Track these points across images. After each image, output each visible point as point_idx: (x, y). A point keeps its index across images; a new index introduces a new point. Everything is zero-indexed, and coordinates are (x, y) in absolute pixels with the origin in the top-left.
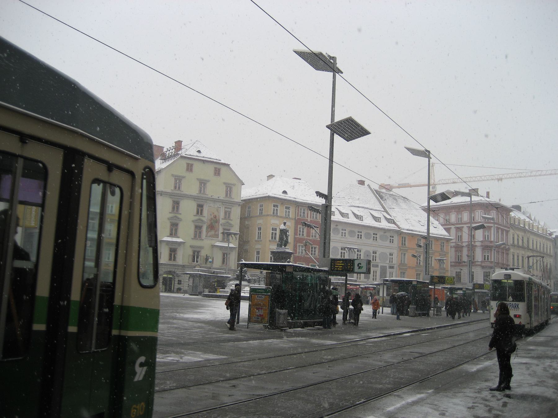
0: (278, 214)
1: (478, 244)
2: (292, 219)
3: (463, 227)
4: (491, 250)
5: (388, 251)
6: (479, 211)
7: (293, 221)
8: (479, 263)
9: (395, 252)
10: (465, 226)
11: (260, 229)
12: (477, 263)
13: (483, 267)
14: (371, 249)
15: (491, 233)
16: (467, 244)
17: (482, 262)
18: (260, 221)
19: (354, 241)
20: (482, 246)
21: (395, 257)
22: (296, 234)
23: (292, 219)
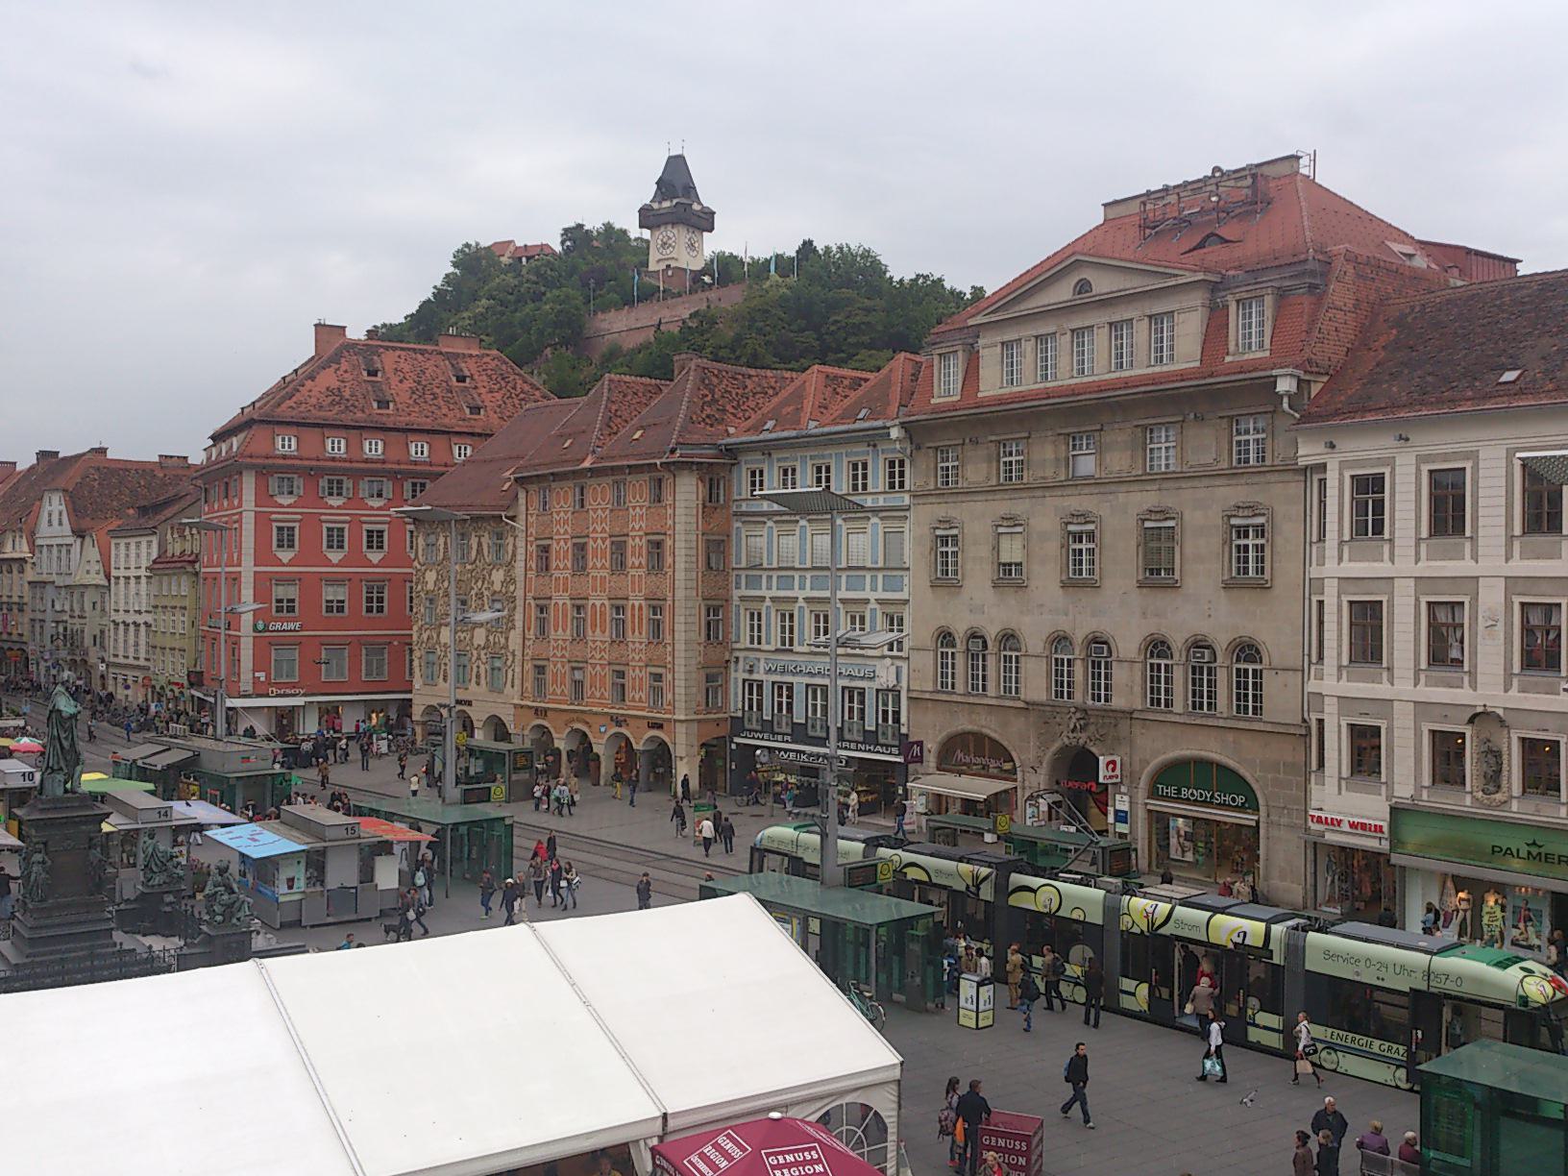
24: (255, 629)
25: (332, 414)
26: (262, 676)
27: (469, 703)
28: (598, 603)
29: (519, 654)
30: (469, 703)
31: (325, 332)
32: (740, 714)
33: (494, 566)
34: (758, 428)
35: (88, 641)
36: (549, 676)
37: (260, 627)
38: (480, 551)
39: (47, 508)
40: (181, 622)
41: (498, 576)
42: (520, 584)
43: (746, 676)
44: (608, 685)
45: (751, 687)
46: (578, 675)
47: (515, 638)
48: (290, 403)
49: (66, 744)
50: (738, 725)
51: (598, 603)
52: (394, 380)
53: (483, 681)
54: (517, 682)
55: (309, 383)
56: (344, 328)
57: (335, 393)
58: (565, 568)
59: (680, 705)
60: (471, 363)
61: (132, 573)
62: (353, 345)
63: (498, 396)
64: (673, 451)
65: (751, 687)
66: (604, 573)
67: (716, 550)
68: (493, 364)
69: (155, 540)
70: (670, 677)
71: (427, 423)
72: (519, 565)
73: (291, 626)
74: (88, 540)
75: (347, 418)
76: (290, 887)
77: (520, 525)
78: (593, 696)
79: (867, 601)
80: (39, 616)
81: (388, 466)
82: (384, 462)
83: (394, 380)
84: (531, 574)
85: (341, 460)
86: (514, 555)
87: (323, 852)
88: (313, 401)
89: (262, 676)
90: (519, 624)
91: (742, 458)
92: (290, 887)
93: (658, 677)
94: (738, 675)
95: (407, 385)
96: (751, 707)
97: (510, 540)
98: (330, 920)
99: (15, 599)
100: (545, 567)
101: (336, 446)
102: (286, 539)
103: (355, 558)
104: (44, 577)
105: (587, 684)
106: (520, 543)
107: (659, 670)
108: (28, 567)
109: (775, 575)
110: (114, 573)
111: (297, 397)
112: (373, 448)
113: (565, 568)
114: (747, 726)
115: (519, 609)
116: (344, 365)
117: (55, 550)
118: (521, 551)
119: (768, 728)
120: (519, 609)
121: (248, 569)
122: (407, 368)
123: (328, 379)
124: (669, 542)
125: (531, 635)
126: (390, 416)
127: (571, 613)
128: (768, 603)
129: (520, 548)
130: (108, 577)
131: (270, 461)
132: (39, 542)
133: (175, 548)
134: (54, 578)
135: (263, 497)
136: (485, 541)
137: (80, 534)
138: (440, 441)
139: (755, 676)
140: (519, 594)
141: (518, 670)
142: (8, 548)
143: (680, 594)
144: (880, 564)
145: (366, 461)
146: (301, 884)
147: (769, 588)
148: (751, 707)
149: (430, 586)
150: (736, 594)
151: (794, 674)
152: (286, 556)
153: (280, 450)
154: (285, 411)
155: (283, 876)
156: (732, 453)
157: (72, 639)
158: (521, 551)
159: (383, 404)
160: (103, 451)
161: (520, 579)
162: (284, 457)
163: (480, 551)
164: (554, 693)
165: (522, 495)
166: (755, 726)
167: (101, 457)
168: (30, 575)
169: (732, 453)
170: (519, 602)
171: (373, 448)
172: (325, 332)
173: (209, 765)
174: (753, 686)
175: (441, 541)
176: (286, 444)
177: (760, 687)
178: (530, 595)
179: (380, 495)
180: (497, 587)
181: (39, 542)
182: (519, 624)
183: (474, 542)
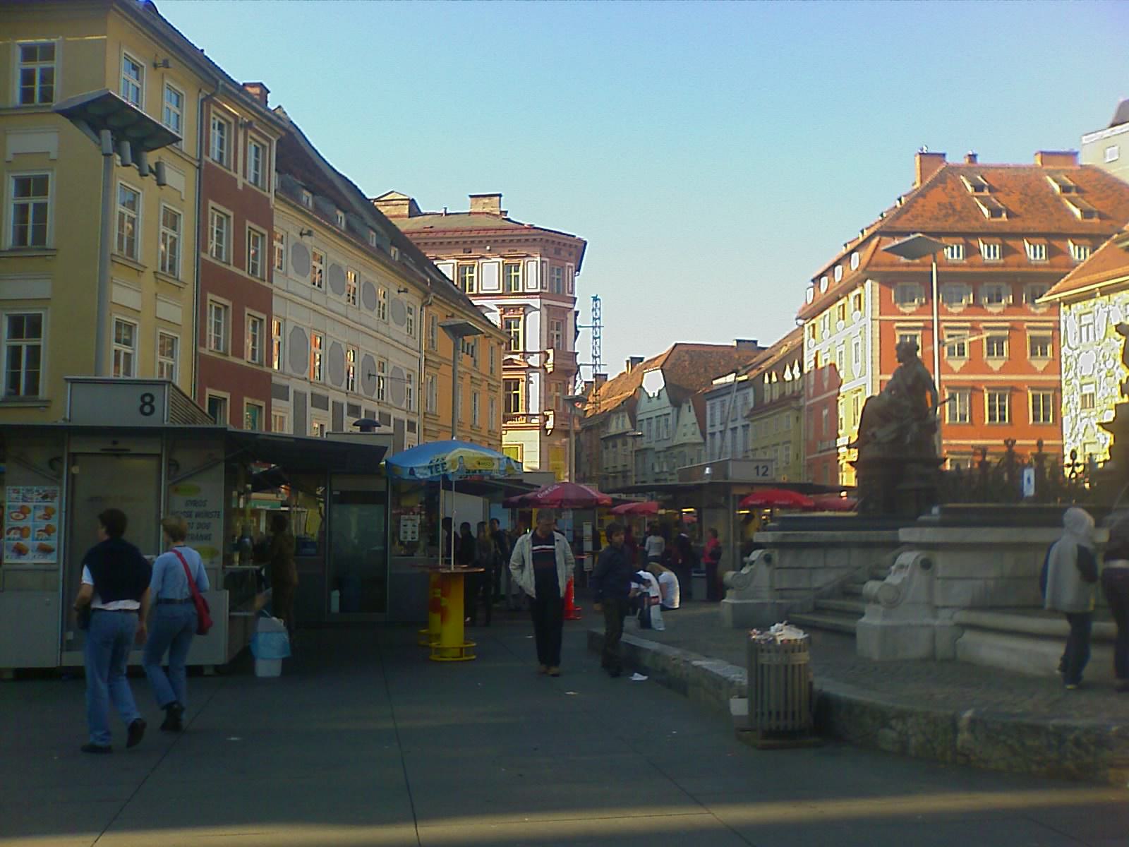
25: (948, 225)
48: (904, 217)
55: (921, 200)
56: (944, 155)
62: (955, 170)
74: (685, 407)
75: (962, 227)
81: (1009, 269)
82: (1003, 266)
99: (620, 468)
110: (709, 430)
117: (654, 420)
130: (703, 434)
132: (639, 418)
134: (653, 445)
181: (639, 418)
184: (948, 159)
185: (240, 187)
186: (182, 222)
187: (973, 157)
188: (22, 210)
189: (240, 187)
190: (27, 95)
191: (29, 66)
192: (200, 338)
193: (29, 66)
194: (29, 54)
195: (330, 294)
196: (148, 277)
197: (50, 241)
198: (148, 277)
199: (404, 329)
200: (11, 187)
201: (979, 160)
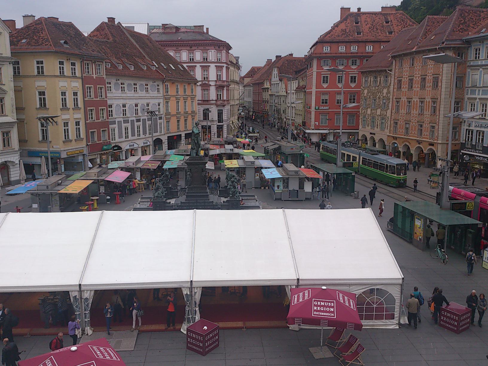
0: (65, 74)
1: (212, 83)
2: (79, 78)
3: (196, 66)
4: (223, 90)
5: (156, 101)
6: (213, 51)
7: (80, 80)
8: (214, 102)
9: (161, 101)
10: (198, 65)
11: (42, 93)
12: (212, 102)
13: (217, 106)
14: (145, 102)
15: (222, 72)
16: (200, 83)
17: (216, 100)
18: (41, 83)
19: (132, 95)
20: (215, 85)
21: (161, 105)
22: (84, 96)
23: (79, 78)
24: (315, 109)
25: (341, 39)
26: (317, 123)
27: (374, 134)
28: (415, 100)
29: (390, 118)
30: (374, 134)
31: (344, 10)
32: (464, 142)
33: (384, 87)
34: (479, 32)
35: (282, 112)
36: (398, 126)
37: (317, 108)
38: (380, 83)
39: (274, 73)
40: (300, 107)
41: (385, 91)
42: (392, 94)
43: (468, 128)
44: (404, 128)
45: (469, 132)
46: (407, 126)
47: (389, 112)
48: (329, 35)
49: (196, 142)
50: (463, 146)
51: (415, 100)
52: (364, 25)
53: (379, 127)
54: (389, 128)
57: (344, 31)
58: (418, 87)
59: (440, 138)
60: (392, 16)
61: (293, 91)
62: (353, 14)
63: (400, 27)
64: (443, 43)
65: (469, 132)
66: (418, 89)
67: (460, 81)
68: (400, 16)
69: (297, 81)
70: (437, 127)
71: (373, 39)
72: (392, 87)
73: (326, 108)
75: (347, 39)
76: (278, 188)
77: (393, 73)
78: (412, 133)
79: (476, 99)
80: (271, 104)
82: (357, 53)
83: (364, 25)
84: (395, 90)
85: (344, 53)
86: (390, 83)
87: (288, 179)
88: (337, 34)
89: (317, 123)
90: (390, 108)
91: (473, 44)
92: (278, 188)
93: (433, 127)
94: (465, 127)
95: (368, 26)
96: (468, 140)
97: (390, 78)
98: (290, 199)
100: (400, 88)
101: (342, 49)
102: (325, 80)
103: (346, 86)
104: (273, 93)
105: (410, 128)
106: (393, 79)
107: (434, 125)
108: (269, 90)
109: (481, 89)
111: (332, 33)
112: (354, 49)
113: (418, 87)
114: (466, 146)
115: (391, 102)
116: (348, 21)
118: (393, 82)
119: (474, 147)
120: (391, 102)
121: (314, 90)
122: (369, 20)
123: (342, 26)
124: (440, 78)
125: (394, 111)
126: (361, 37)
127: (419, 104)
128: (478, 100)
129: (392, 81)
130: (287, 93)
131: (321, 55)
133: (302, 84)
134: (275, 93)
135: (319, 67)
136: (382, 79)
137: (281, 80)
138: (334, 46)
139: (471, 128)
140: (391, 97)
141: (389, 123)
142: (265, 85)
143: (443, 97)
144: (481, 86)
145: (352, 53)
146: (281, 187)
147: (479, 94)
148: (468, 140)
149: (365, 95)
150: (466, 97)
151: (485, 128)
152: (325, 85)
153: (325, 51)
154: (327, 39)
155: (276, 185)
156: (469, 42)
157: (278, 111)
158: (393, 82)
159: (359, 33)
160: (292, 55)
161: (392, 92)
162: (326, 53)
163: (380, 83)
164: (399, 132)
165: (394, 62)
166: (469, 147)
167: (291, 57)
168: (270, 93)
169: (469, 42)
170: (391, 100)
171: (354, 49)
172: (344, 10)
173: (283, 150)
174: (469, 132)
175: (369, 80)
176: (326, 49)
177: (472, 132)
178: (394, 97)
179: (343, 65)
180: (385, 95)
182: (390, 108)
183: (379, 79)
184: (351, 11)
185: (95, 78)
186: (78, 94)
187: (359, 9)
188: (40, 99)
189: (95, 78)
190: (39, 72)
191: (38, 65)
192: (86, 119)
193: (38, 65)
194: (38, 63)
195: (127, 92)
196: (71, 110)
197: (47, 107)
198: (71, 110)
199: (156, 92)
200: (37, 94)
201: (362, 11)
